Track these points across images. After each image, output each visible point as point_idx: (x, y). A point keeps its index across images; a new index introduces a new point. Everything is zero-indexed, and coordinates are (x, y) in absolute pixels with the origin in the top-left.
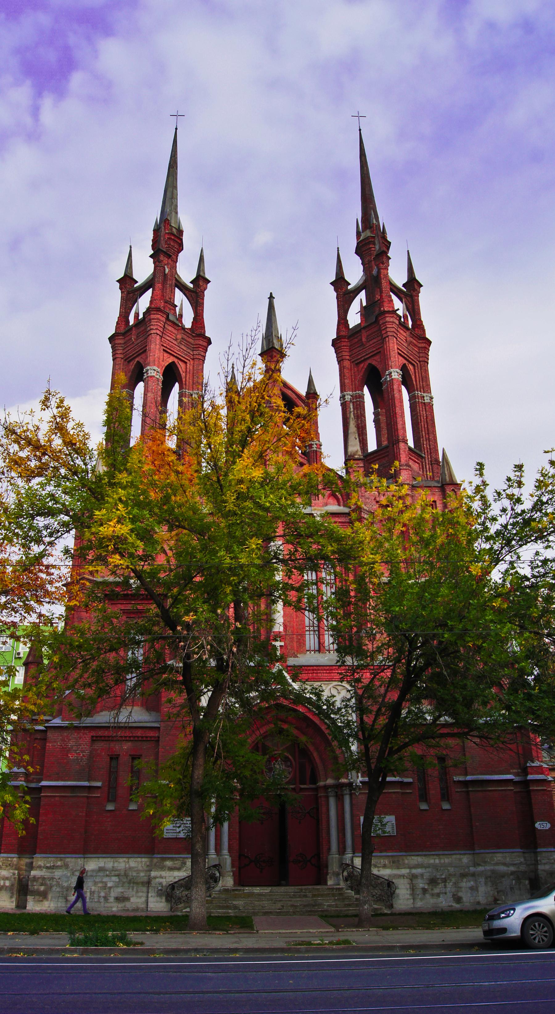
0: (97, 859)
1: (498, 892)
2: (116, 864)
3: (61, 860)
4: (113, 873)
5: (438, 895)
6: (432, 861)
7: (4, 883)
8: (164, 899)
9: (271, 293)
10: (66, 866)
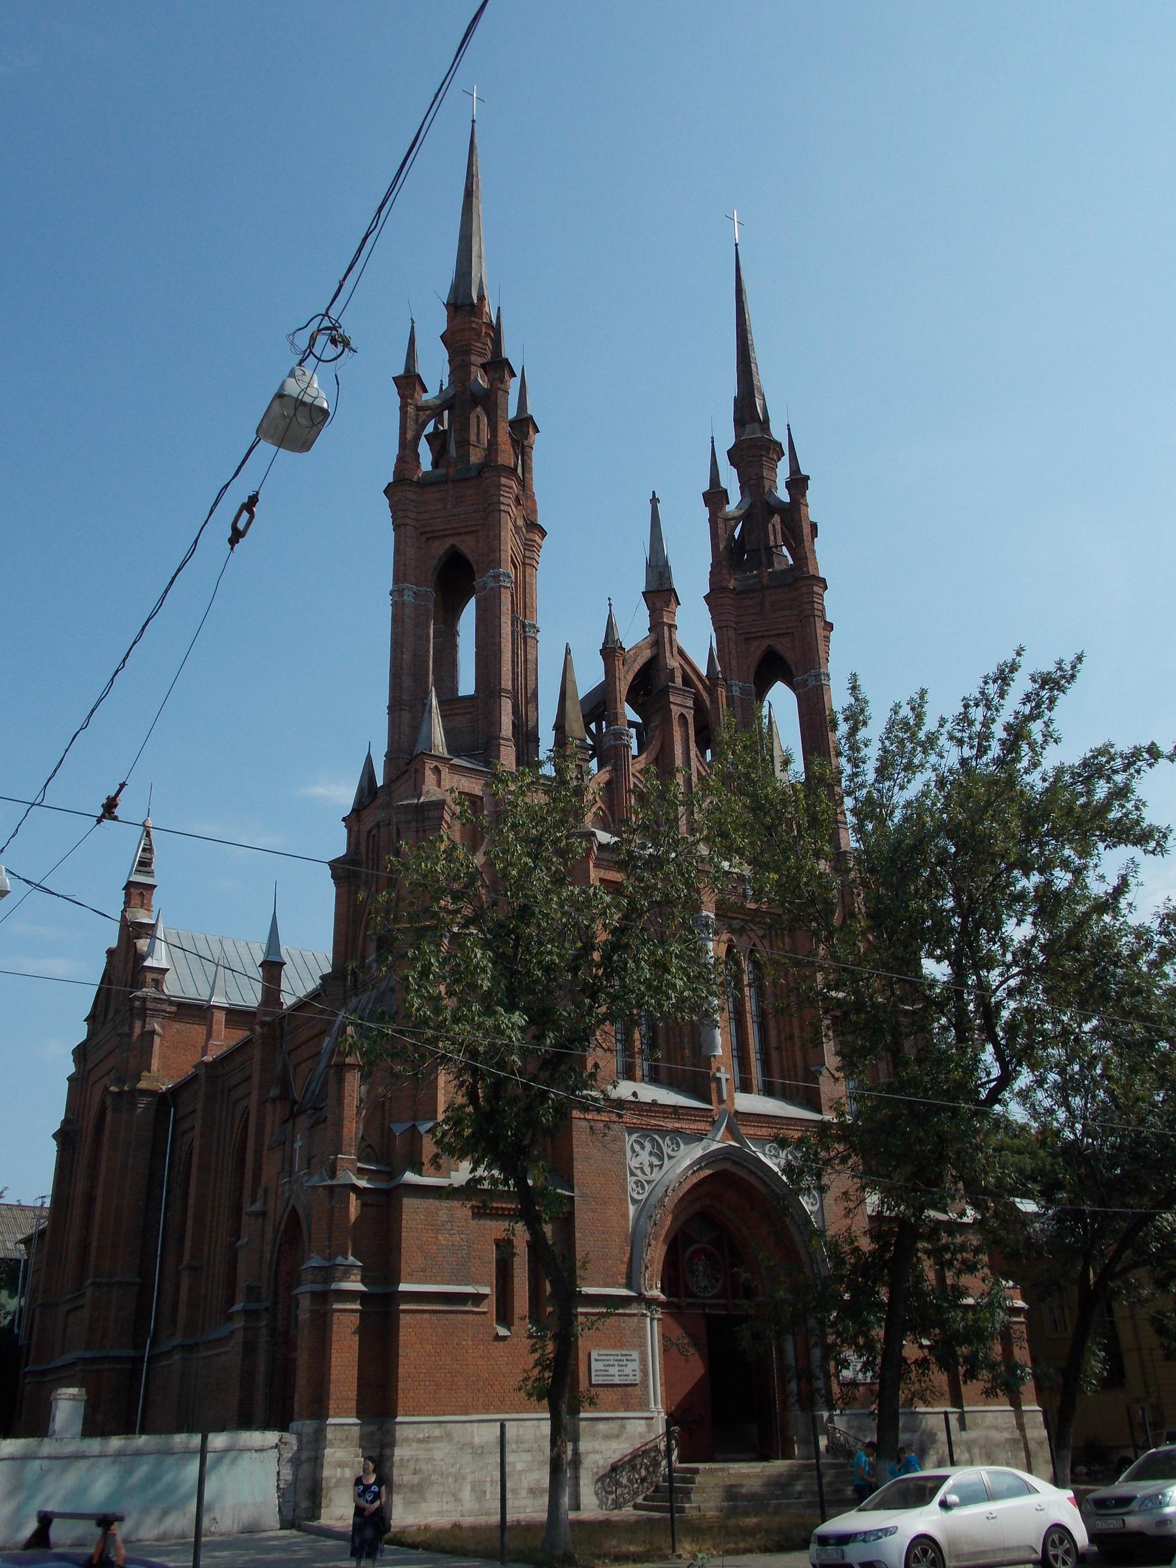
7: (343, 1473)
10: (449, 1436)
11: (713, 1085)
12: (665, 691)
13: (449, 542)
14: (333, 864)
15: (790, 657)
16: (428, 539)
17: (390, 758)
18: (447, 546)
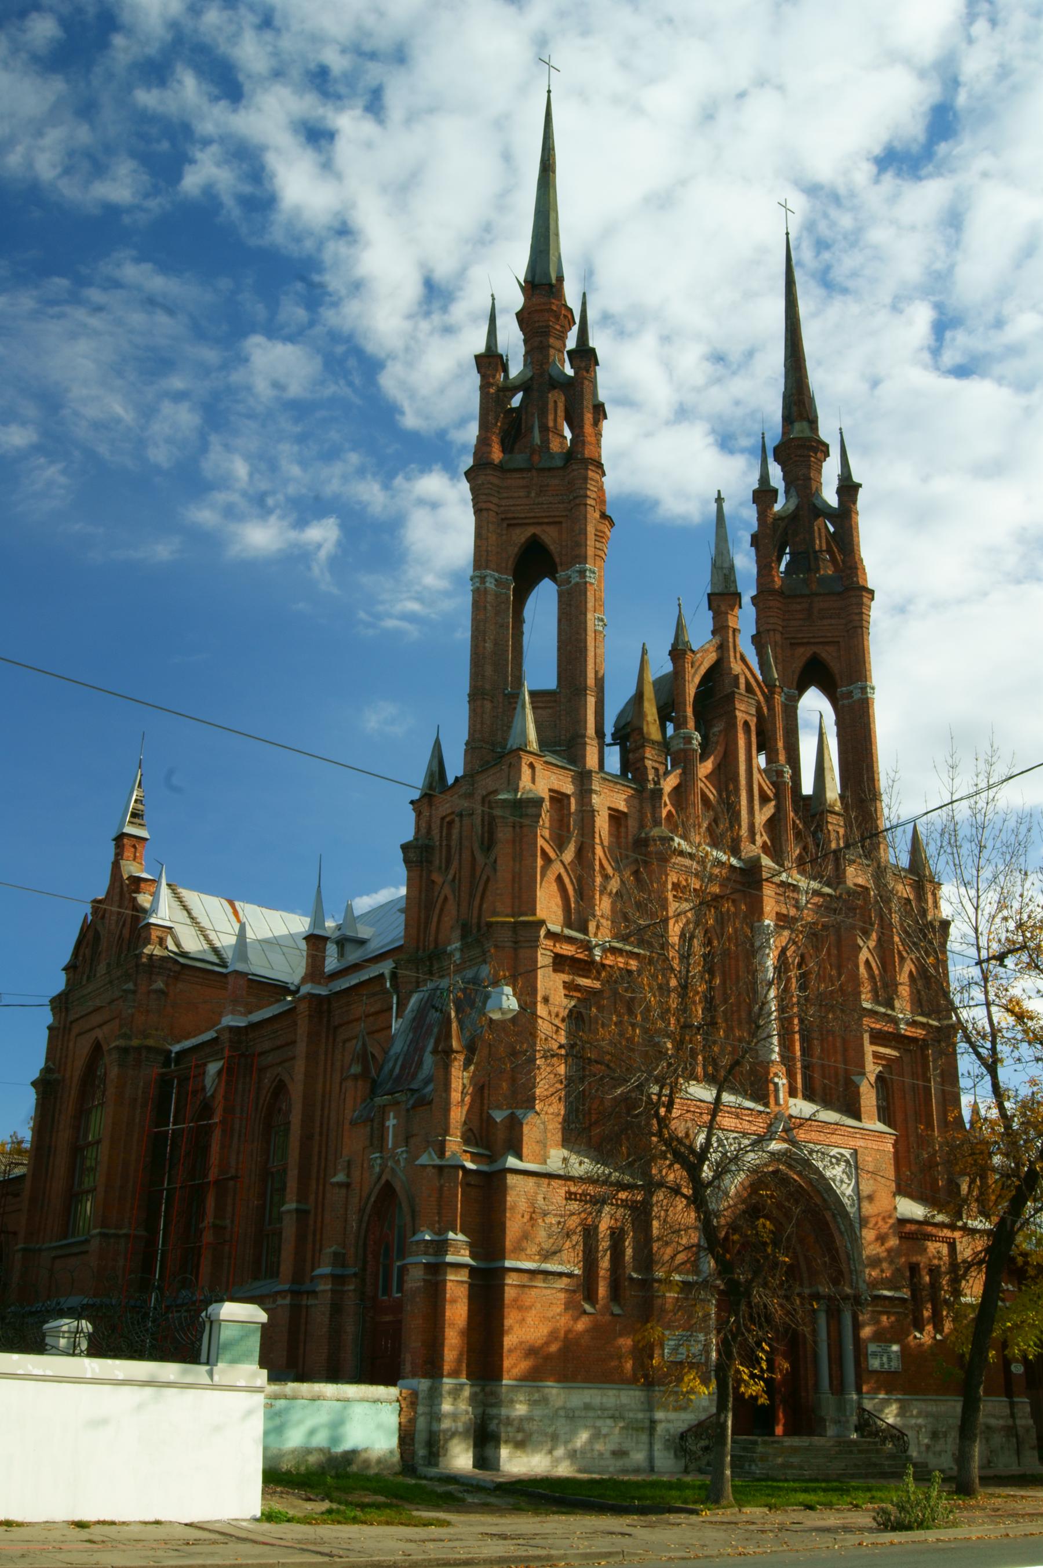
0: (580, 1391)
1: (991, 1452)
2: (605, 1400)
3: (538, 1391)
4: (606, 1413)
5: (940, 1453)
6: (929, 1409)
8: (672, 1455)
9: (719, 491)
11: (771, 1087)
12: (730, 698)
13: (530, 531)
14: (405, 848)
15: (835, 666)
16: (509, 525)
17: (472, 747)
18: (529, 534)
